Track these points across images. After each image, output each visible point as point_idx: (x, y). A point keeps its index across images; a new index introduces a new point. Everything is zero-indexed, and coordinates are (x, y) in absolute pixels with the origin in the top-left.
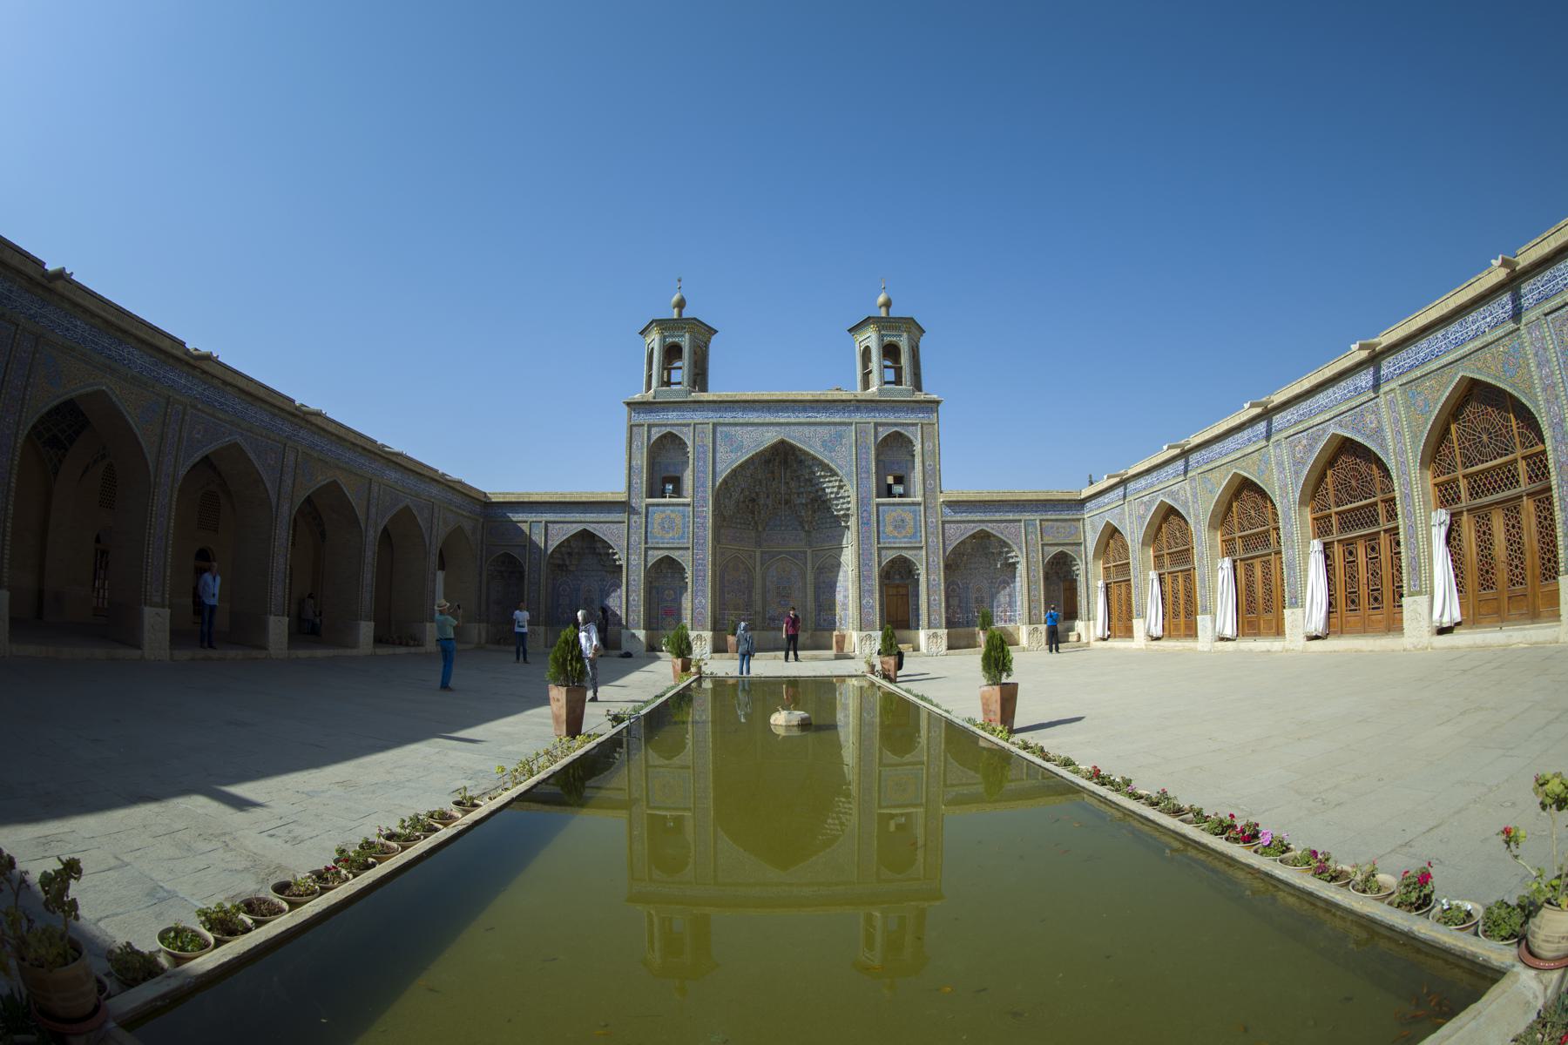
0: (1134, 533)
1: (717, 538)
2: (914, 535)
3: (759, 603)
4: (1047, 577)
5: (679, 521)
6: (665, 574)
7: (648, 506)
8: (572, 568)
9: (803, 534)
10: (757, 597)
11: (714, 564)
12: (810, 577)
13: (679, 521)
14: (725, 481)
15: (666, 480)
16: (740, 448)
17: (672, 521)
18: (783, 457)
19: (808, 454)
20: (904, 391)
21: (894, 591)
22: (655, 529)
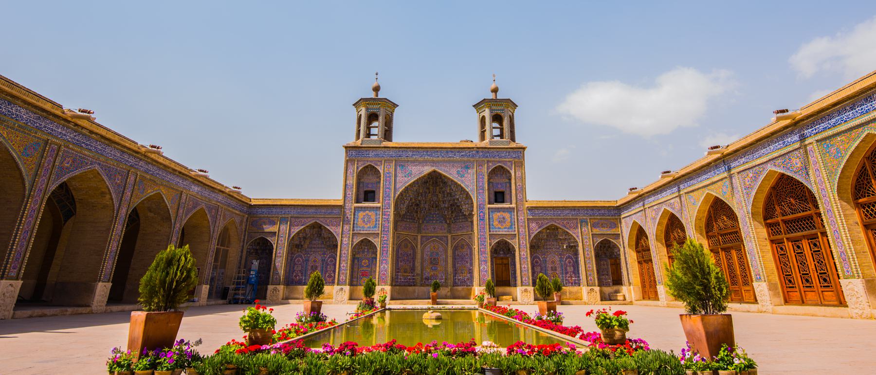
0: (652, 230)
1: (396, 228)
2: (511, 227)
3: (419, 268)
4: (597, 256)
5: (373, 217)
6: (365, 248)
7: (355, 208)
8: (306, 246)
9: (446, 226)
10: (418, 264)
11: (393, 244)
12: (450, 252)
13: (373, 217)
14: (401, 194)
16: (410, 175)
17: (369, 217)
18: (435, 180)
20: (505, 143)
21: (499, 262)
22: (360, 222)
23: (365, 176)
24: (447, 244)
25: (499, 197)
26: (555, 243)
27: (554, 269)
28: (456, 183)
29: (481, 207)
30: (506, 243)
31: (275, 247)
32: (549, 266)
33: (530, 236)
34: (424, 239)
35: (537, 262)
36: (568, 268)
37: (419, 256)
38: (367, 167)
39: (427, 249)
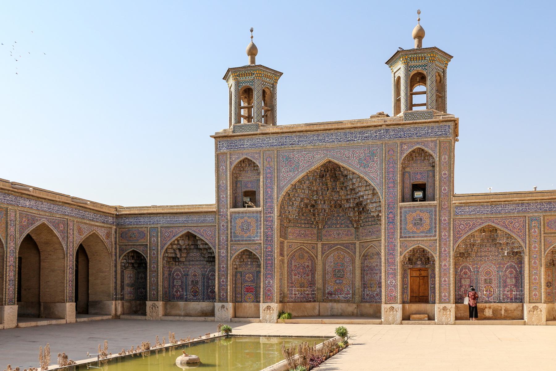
3: (320, 281)
9: (353, 230)
15: (246, 194)
17: (249, 224)
18: (332, 173)
19: (350, 171)
22: (238, 231)
23: (243, 173)
24: (355, 253)
25: (419, 190)
26: (493, 249)
27: (488, 282)
28: (359, 177)
29: (390, 207)
30: (424, 250)
31: (148, 262)
32: (482, 278)
33: (455, 241)
34: (326, 247)
35: (465, 273)
36: (508, 280)
37: (319, 268)
38: (243, 161)
39: (331, 259)
